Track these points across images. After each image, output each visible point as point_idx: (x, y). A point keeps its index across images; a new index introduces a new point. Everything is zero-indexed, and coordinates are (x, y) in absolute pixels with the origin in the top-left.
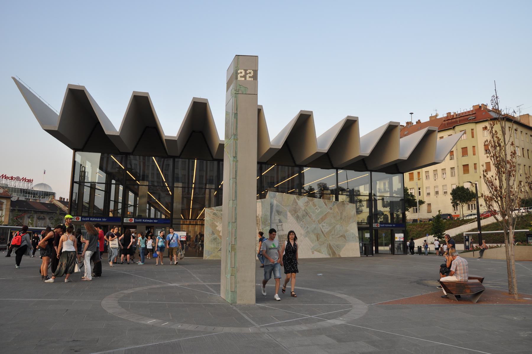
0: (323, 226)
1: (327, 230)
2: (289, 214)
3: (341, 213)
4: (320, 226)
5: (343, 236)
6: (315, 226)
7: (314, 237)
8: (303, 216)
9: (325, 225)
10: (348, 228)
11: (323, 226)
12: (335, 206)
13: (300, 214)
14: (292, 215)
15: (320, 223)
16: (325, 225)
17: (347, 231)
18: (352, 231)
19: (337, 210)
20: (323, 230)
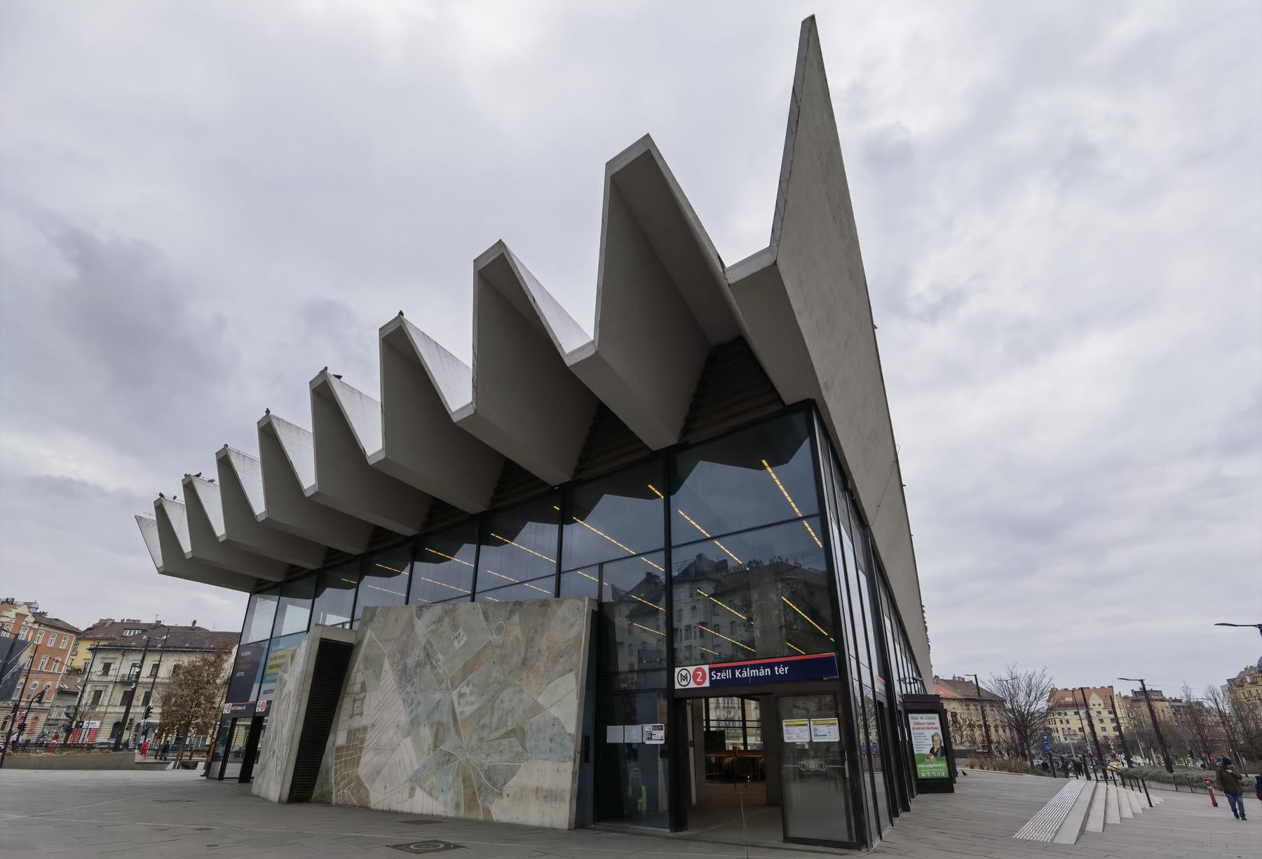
0: (461, 695)
1: (469, 710)
2: (387, 665)
3: (530, 642)
4: (455, 694)
5: (518, 733)
6: (438, 696)
7: (426, 733)
8: (419, 665)
9: (466, 690)
10: (541, 700)
11: (461, 695)
12: (516, 619)
13: (410, 662)
14: (392, 665)
15: (454, 687)
16: (466, 690)
17: (536, 709)
18: (554, 712)
19: (517, 631)
20: (458, 710)
